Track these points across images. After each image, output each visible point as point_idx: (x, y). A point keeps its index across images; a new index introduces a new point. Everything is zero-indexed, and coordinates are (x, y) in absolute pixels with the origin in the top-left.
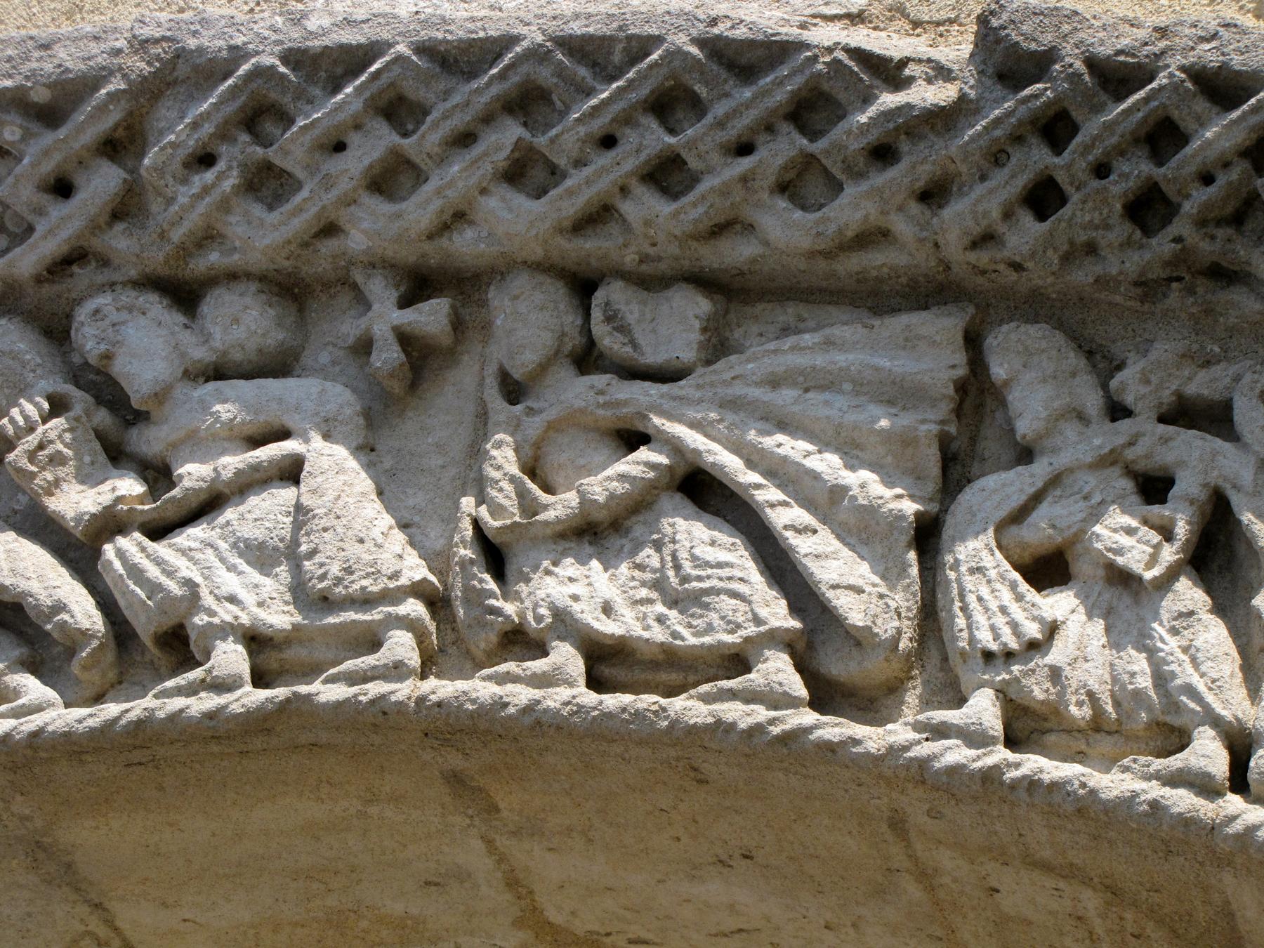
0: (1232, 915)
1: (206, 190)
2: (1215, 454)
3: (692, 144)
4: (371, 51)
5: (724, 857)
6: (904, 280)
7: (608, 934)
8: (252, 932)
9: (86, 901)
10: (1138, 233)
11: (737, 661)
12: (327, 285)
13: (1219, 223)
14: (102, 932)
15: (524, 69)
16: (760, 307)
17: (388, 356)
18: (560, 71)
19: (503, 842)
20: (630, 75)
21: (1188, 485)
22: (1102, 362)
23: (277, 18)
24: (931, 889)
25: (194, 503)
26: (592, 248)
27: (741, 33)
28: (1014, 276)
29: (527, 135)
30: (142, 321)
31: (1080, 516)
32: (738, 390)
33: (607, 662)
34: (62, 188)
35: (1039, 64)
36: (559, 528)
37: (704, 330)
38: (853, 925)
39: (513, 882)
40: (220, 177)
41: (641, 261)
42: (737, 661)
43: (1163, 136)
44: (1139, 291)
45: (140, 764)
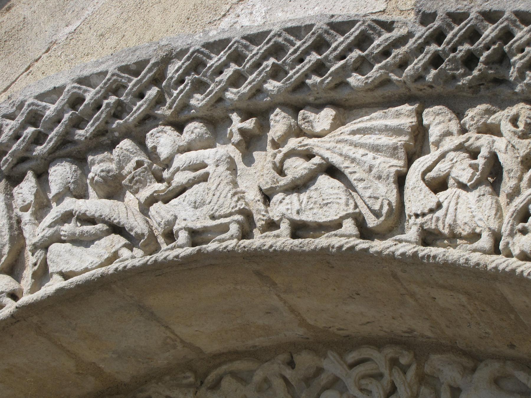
0: (505, 298)
1: (181, 91)
2: (494, 142)
3: (326, 57)
4: (228, 40)
5: (351, 295)
6: (397, 96)
7: (330, 328)
8: (219, 334)
9: (163, 326)
10: (467, 70)
11: (338, 225)
12: (222, 119)
13: (493, 63)
14: (172, 336)
15: (273, 40)
16: (354, 111)
17: (237, 137)
18: (286, 40)
19: (282, 295)
20: (306, 37)
21: (484, 152)
22: (460, 115)
23: (201, 34)
24: (416, 300)
25: (178, 190)
26: (299, 97)
27: (340, 19)
28: (430, 90)
29: (276, 61)
30: (165, 135)
31: (449, 167)
32: (342, 137)
33: (299, 229)
34: (141, 96)
35: (433, 16)
36: (285, 187)
37: (333, 119)
38: (401, 317)
39: (292, 310)
40: (186, 86)
41: (315, 99)
42: (338, 225)
43: (473, 35)
44: (471, 90)
45: (160, 275)
